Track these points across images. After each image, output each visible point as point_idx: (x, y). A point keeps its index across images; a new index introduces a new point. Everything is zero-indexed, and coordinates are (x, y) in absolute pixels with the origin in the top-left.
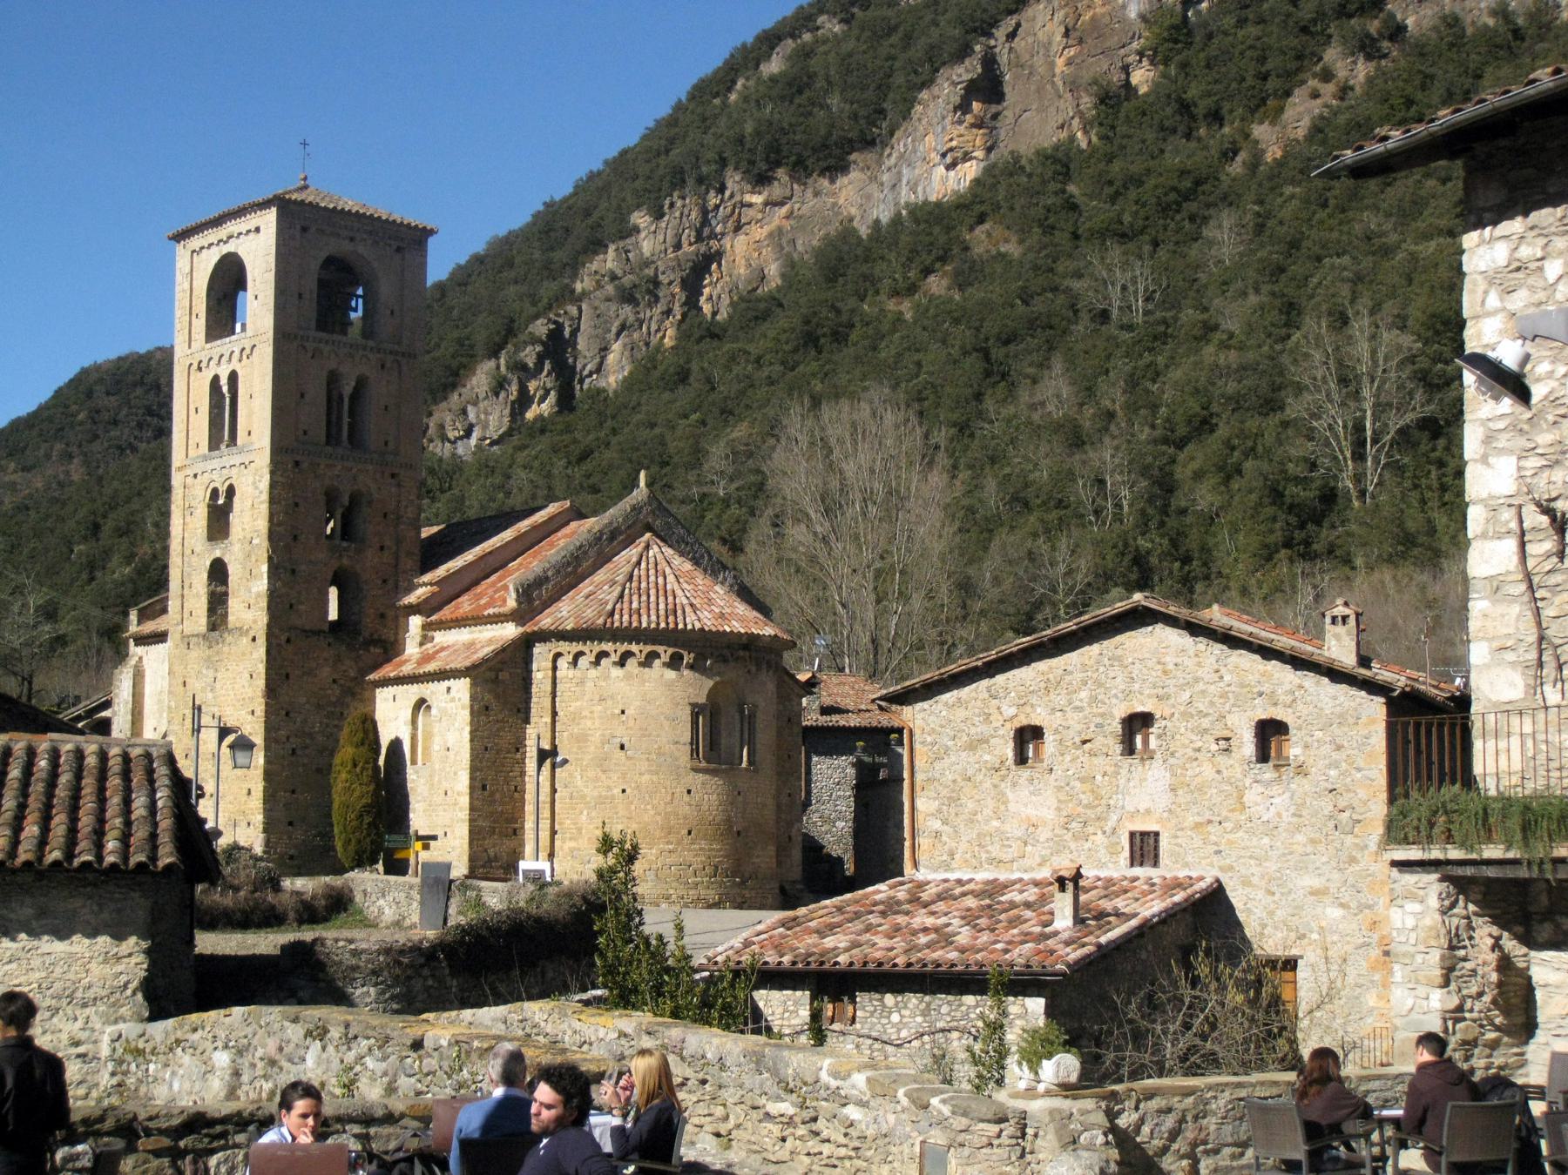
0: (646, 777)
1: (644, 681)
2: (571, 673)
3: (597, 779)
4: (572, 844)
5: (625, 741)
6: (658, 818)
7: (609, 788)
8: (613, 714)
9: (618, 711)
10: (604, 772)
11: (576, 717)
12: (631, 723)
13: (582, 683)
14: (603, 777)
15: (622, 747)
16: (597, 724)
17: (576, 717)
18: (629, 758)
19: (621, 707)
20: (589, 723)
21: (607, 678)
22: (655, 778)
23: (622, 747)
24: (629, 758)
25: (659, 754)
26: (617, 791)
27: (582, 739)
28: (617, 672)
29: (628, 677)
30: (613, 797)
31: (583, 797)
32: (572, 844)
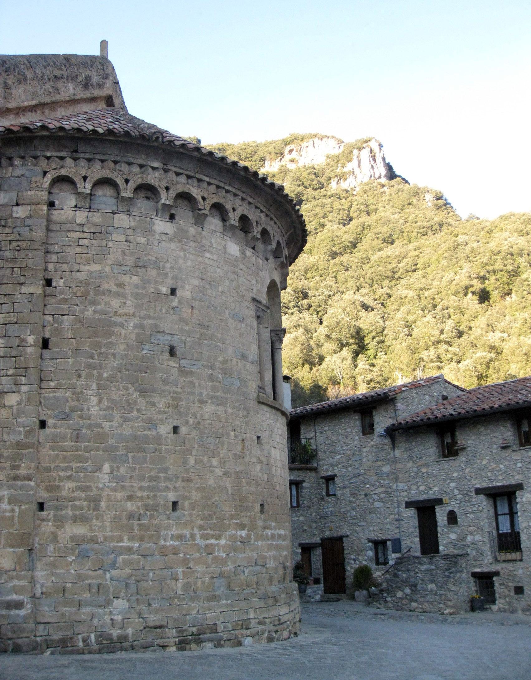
0: (209, 409)
1: (202, 249)
2: (81, 217)
3: (129, 405)
4: (80, 530)
5: (175, 341)
6: (227, 482)
7: (152, 424)
8: (158, 294)
9: (165, 290)
10: (143, 392)
11: (91, 291)
12: (186, 312)
13: (101, 233)
14: (142, 402)
15: (172, 352)
16: (130, 306)
17: (91, 291)
18: (183, 372)
19: (170, 283)
20: (115, 303)
21: (148, 232)
22: (221, 409)
23: (172, 352)
24: (183, 372)
25: (225, 371)
26: (164, 429)
27: (103, 328)
28: (161, 225)
29: (181, 236)
30: (158, 439)
31: (102, 437)
32: (80, 530)
